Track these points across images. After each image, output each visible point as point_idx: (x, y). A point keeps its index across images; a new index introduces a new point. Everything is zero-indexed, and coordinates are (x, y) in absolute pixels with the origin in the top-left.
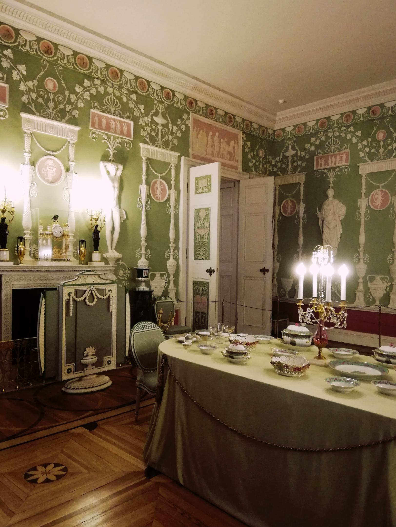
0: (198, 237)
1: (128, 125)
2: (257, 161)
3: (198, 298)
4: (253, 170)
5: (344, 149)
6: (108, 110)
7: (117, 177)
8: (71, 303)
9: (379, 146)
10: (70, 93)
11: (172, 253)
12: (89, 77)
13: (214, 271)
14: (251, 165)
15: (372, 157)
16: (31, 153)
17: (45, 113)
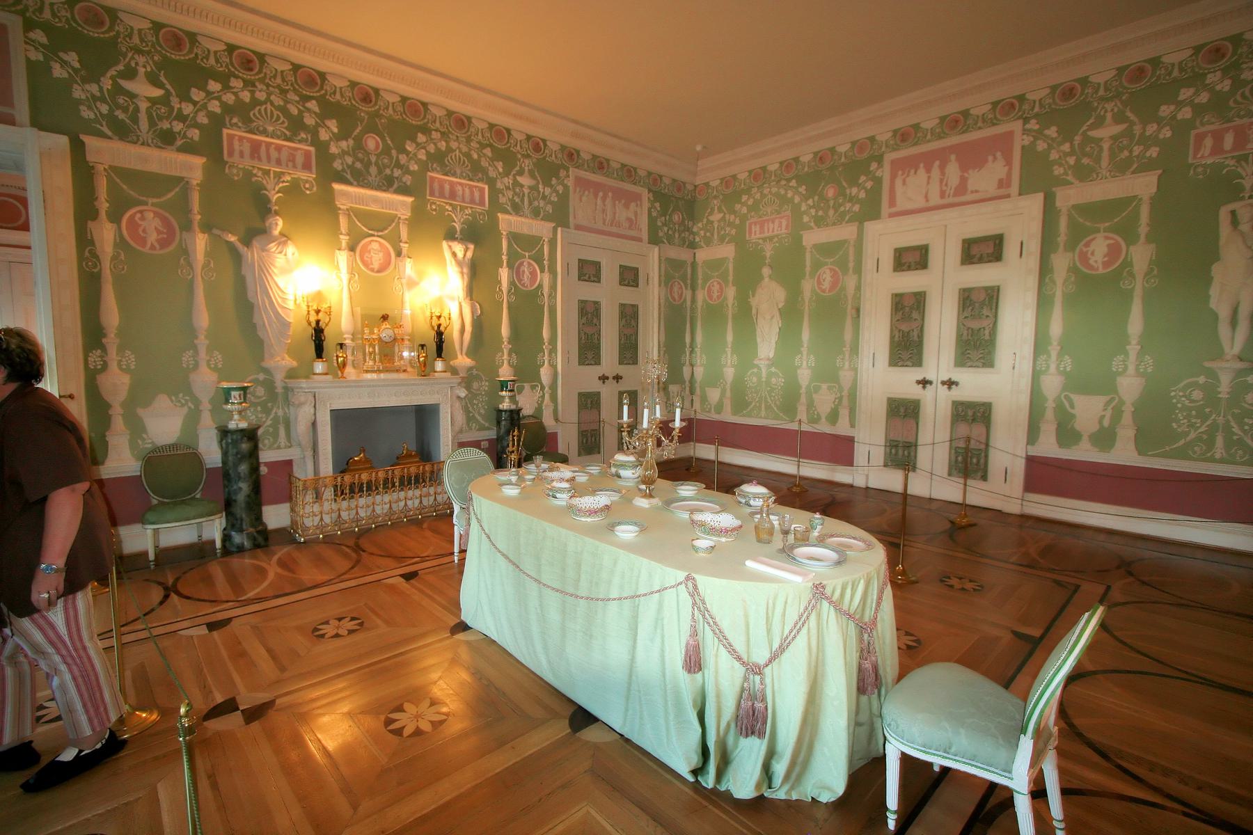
1: (482, 191)
12: (426, 130)
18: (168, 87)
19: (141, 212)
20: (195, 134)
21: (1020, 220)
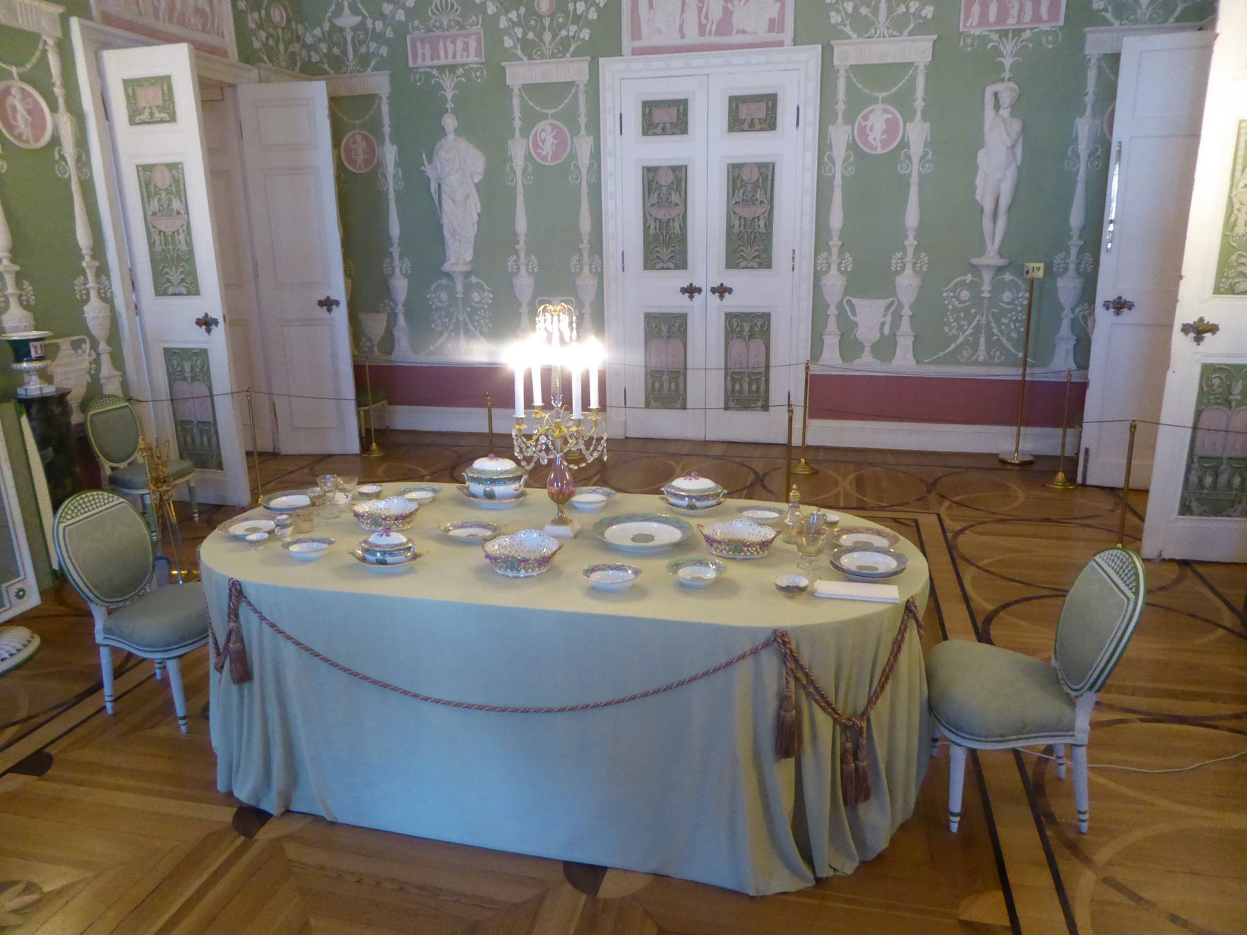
2: (272, 36)
3: (183, 388)
4: (265, 58)
9: (543, 29)
11: (91, 284)
13: (216, 322)
14: (257, 45)
15: (530, 49)
21: (793, 75)
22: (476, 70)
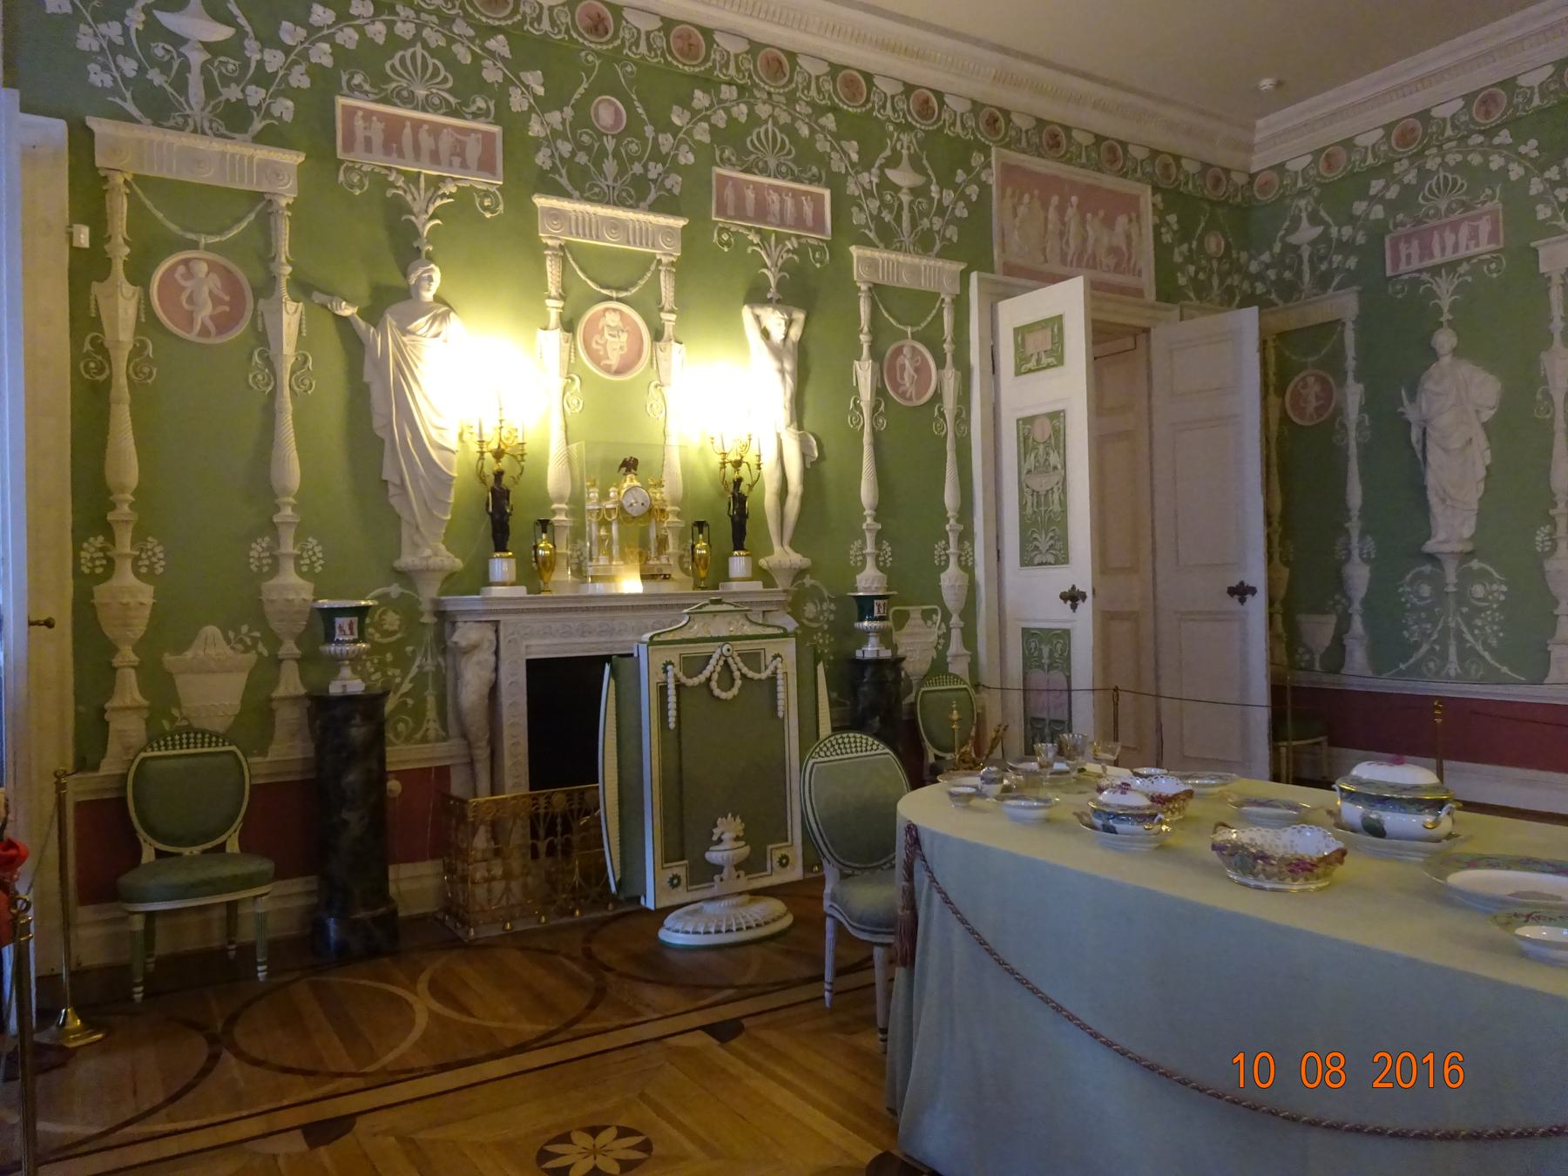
0: (1029, 498)
3: (1038, 677)
4: (1192, 295)
5: (1484, 203)
6: (761, 164)
7: (789, 343)
8: (672, 692)
10: (657, 132)
11: (952, 549)
12: (708, 83)
13: (1083, 596)
14: (1182, 281)
16: (562, 297)
17: (596, 190)
18: (242, 21)
19: (186, 262)
20: (285, 108)
22: (1489, 262)
